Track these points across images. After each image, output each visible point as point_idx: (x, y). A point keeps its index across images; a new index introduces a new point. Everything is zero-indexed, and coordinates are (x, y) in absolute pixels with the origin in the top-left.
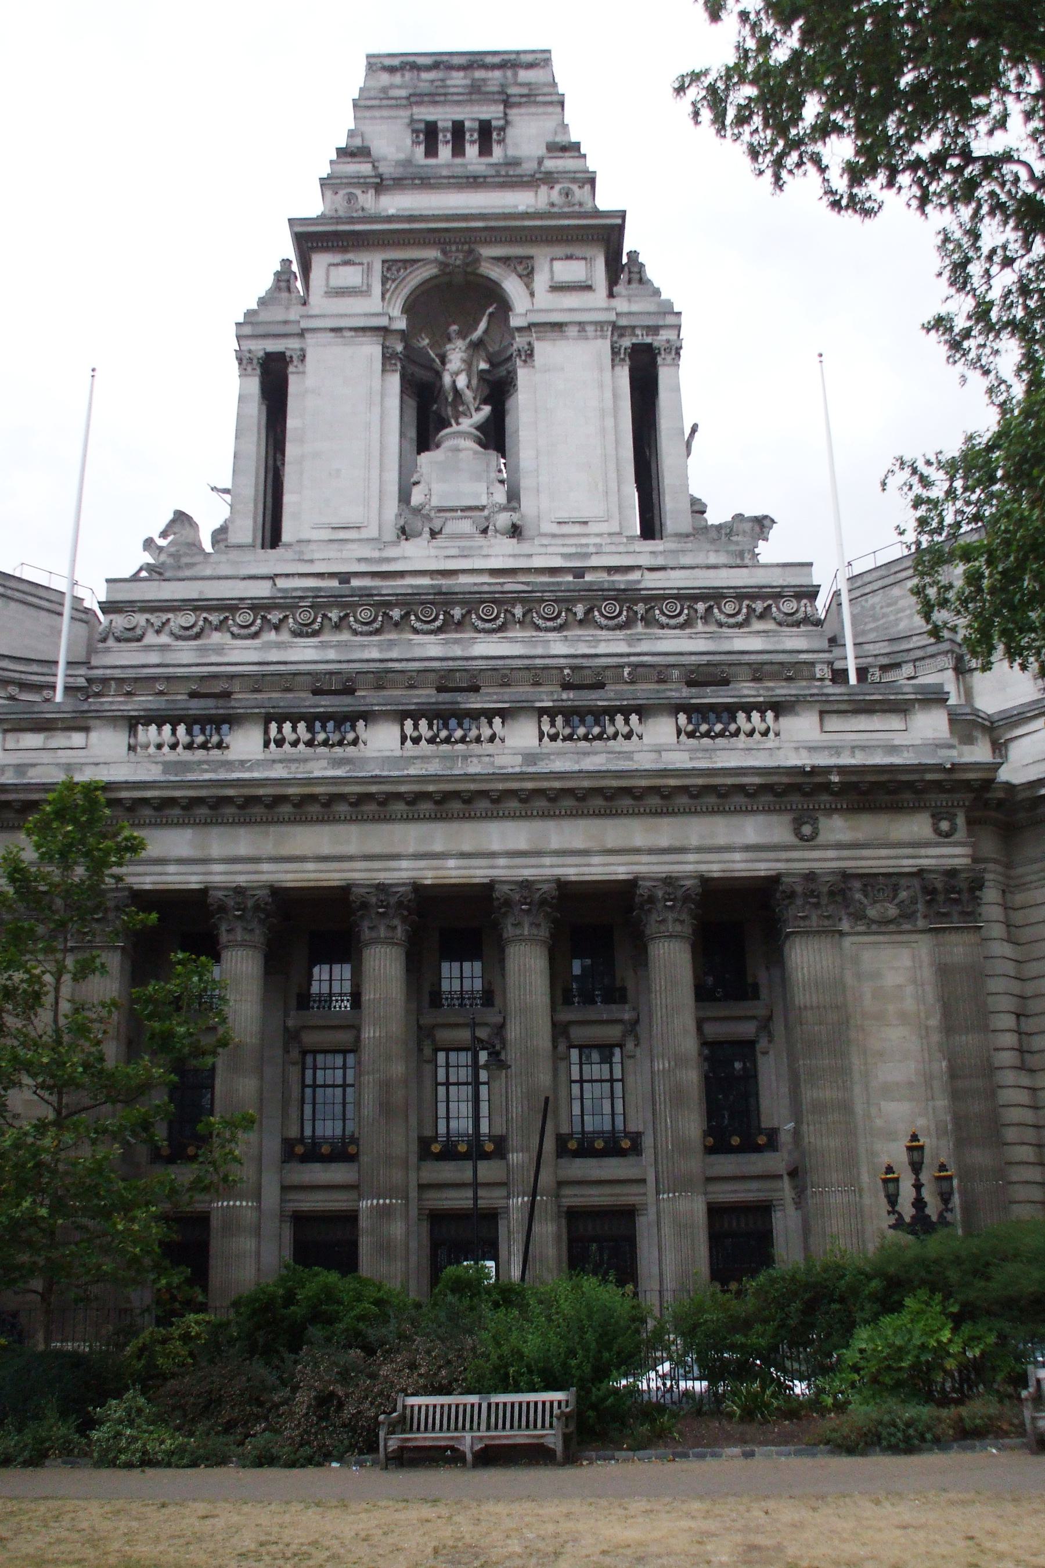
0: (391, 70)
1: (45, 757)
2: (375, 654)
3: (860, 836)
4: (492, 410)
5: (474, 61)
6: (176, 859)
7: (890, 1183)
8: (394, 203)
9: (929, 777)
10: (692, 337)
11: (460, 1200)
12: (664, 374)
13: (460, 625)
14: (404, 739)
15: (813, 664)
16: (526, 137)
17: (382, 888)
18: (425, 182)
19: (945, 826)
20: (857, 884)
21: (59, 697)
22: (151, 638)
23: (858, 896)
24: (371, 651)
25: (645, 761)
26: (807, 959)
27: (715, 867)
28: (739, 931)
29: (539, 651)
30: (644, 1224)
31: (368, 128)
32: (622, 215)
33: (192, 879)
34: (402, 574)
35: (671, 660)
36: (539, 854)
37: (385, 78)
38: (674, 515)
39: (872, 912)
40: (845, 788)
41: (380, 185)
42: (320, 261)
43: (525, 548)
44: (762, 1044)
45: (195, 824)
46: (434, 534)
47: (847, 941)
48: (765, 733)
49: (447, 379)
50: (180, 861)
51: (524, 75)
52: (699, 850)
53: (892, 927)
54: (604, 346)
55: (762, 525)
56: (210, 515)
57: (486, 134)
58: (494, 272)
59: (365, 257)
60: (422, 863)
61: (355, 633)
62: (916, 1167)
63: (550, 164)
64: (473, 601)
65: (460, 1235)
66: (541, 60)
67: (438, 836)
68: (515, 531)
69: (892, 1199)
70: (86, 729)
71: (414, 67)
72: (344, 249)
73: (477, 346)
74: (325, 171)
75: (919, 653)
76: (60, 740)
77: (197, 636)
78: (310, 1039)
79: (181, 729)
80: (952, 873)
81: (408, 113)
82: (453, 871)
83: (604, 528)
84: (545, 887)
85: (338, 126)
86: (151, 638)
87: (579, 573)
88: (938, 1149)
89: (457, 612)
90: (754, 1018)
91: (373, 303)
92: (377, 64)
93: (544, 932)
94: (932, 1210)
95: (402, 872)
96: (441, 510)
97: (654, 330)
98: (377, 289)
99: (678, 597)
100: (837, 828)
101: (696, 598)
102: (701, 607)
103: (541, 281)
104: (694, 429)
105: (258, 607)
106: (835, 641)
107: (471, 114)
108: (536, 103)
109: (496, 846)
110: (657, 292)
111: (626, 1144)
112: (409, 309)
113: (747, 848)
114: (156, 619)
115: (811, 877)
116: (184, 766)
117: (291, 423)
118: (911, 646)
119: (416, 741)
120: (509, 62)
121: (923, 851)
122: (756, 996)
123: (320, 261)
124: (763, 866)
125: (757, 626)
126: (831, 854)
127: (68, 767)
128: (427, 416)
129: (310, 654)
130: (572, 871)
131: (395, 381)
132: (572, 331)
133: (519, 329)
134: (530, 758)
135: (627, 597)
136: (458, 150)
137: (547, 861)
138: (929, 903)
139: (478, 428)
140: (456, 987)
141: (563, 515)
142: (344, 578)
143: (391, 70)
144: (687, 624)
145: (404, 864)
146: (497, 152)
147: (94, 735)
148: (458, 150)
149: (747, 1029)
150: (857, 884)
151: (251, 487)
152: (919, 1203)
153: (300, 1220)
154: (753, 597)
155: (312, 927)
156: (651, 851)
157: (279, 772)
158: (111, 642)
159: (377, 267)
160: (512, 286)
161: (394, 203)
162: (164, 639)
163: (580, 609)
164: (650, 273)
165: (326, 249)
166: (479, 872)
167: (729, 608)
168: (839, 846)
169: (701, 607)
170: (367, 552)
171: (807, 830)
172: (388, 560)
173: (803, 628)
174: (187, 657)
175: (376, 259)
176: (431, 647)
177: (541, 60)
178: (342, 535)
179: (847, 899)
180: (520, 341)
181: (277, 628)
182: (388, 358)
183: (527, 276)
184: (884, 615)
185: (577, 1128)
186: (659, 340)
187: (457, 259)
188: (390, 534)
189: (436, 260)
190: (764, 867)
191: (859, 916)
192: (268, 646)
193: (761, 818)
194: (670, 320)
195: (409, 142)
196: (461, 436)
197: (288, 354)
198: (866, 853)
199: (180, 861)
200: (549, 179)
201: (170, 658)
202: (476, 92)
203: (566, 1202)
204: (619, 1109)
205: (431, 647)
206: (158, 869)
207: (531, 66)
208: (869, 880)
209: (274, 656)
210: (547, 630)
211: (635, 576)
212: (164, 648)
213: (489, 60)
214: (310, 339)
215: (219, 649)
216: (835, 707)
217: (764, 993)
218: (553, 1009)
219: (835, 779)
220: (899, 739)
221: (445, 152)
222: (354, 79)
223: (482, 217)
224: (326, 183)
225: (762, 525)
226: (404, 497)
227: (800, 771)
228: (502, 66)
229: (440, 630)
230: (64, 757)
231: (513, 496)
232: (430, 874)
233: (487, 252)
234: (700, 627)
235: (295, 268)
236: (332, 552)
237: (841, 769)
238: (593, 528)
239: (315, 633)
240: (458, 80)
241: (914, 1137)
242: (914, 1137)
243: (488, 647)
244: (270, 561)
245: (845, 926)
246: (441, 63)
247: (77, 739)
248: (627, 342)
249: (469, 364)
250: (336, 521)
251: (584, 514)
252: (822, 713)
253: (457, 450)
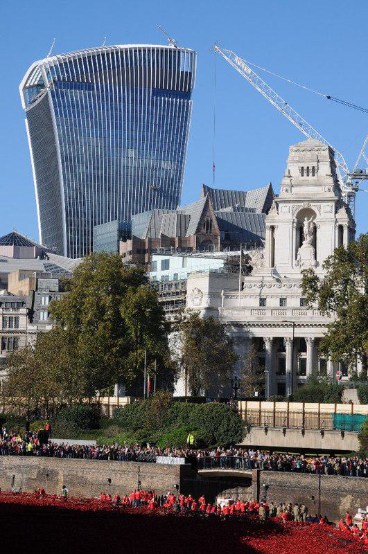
49: (304, 230)
107: (311, 165)
123: (280, 205)
131: (294, 232)
136: (308, 175)
146: (316, 174)
148: (308, 175)
221: (305, 174)
230: (241, 315)
231: (316, 258)
233: (312, 204)
248: (337, 224)
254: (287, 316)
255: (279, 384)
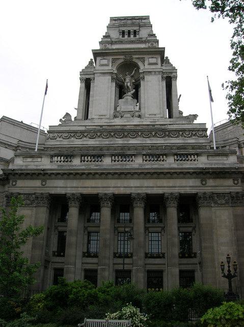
0: (115, 20)
1: (32, 163)
2: (107, 143)
3: (216, 184)
4: (136, 91)
5: (133, 18)
6: (60, 187)
7: (222, 266)
8: (115, 47)
9: (232, 170)
10: (180, 74)
11: (120, 267)
12: (173, 82)
13: (126, 137)
14: (112, 160)
15: (206, 146)
16: (143, 33)
17: (105, 194)
18: (121, 42)
19: (236, 182)
20: (216, 195)
21: (36, 150)
22: (58, 139)
23: (216, 198)
24: (106, 142)
25: (167, 166)
26: (203, 212)
27: (182, 191)
28: (188, 205)
29: (144, 143)
30: (165, 274)
31: (110, 32)
32: (164, 48)
33: (63, 191)
34: (114, 125)
35: (173, 145)
36: (142, 187)
37: (114, 22)
38: (175, 114)
39: (219, 202)
40: (213, 173)
41: (112, 43)
42: (98, 59)
43: (142, 120)
44: (193, 233)
45: (64, 179)
46: (122, 117)
47: (213, 208)
48: (195, 160)
49: (126, 84)
50: (60, 187)
51: (143, 21)
52: (179, 187)
53: (223, 206)
54: (160, 76)
55: (195, 116)
56: (74, 114)
57: (135, 33)
58: (136, 61)
59: (108, 58)
60: (115, 189)
61: (103, 138)
62: (229, 262)
63: (148, 38)
64: (130, 131)
65: (123, 275)
66: (147, 18)
67: (119, 183)
68: (140, 116)
69: (223, 270)
70: (41, 157)
71: (120, 20)
72: (104, 56)
73: (132, 77)
74: (100, 40)
75: (230, 144)
76: (35, 160)
77: (68, 138)
78: (90, 229)
79: (62, 158)
80: (237, 193)
82: (122, 191)
83: (159, 116)
84: (143, 195)
85: (103, 31)
86: (58, 139)
87: (154, 125)
88: (234, 258)
89: (126, 134)
90: (191, 227)
91: (110, 67)
92: (112, 19)
93: (143, 205)
94: (232, 272)
95: (110, 191)
96: (123, 112)
97: (171, 73)
98: (111, 65)
99: (175, 131)
100: (211, 182)
101: (180, 131)
102: (181, 133)
103: (146, 63)
104: (180, 96)
105: (82, 132)
106: (212, 141)
107: (132, 29)
108: (146, 26)
109: (132, 185)
110: (172, 65)
111: (161, 255)
112: (118, 69)
113: (190, 187)
114: (60, 135)
115: (205, 193)
116: (62, 166)
117: (91, 93)
119: (115, 161)
120: (141, 18)
121: (231, 188)
122: (192, 222)
123: (98, 59)
124: (194, 191)
125: (193, 137)
126: (210, 188)
127: (37, 166)
128: (121, 91)
129: (93, 143)
130: (149, 191)
131: (114, 84)
133: (141, 73)
134: (140, 165)
135: (164, 131)
136: (129, 36)
137: (144, 189)
138: (232, 200)
139: (133, 94)
140: (123, 218)
141: (150, 113)
142: (101, 126)
143: (115, 20)
144: (177, 137)
145: (111, 189)
146: (138, 36)
147: (43, 159)
148: (129, 36)
149: (190, 229)
150: (216, 195)
151: (82, 107)
152: (229, 271)
153: (86, 271)
154: (193, 131)
155: (90, 204)
156: (168, 187)
157: (83, 167)
158: (49, 140)
159: (111, 60)
160: (140, 64)
161: (115, 47)
162: (61, 139)
163: (153, 133)
164: (170, 61)
165: (100, 56)
166: (128, 191)
167: (187, 133)
168: (212, 186)
169: (181, 133)
170: (107, 121)
171: (204, 183)
172: (111, 122)
173: (204, 138)
174: (65, 143)
175: (110, 58)
176: (120, 141)
177: (147, 18)
178: (102, 117)
179: (213, 198)
180: (141, 76)
181: (86, 137)
182: (113, 79)
183: (143, 62)
185: (119, 251)
186: (172, 75)
187: (128, 58)
188: (112, 117)
189: (124, 58)
190: (194, 191)
191: (216, 203)
192: (84, 141)
193: (193, 180)
194: (175, 71)
196: (128, 97)
198: (217, 188)
199: (60, 187)
200: (148, 41)
201: (62, 143)
202: (133, 25)
203: (147, 269)
204: (119, 245)
205: (120, 141)
206: (56, 189)
207: (145, 19)
208: (218, 195)
209: (85, 143)
210: (146, 138)
211: (166, 126)
212: (61, 141)
213: (136, 18)
214: (96, 75)
215: (73, 141)
216: (211, 154)
217: (194, 221)
218: (145, 224)
220: (225, 162)
221: (126, 37)
222: (107, 22)
223: (134, 49)
224: (100, 43)
225: (195, 116)
226: (115, 109)
227: (203, 169)
228: (139, 19)
229: (122, 138)
230: (36, 163)
232: (117, 191)
233: (134, 56)
234: (181, 138)
235: (93, 61)
236: (99, 121)
237: (212, 168)
238: (157, 116)
239: (94, 138)
240: (129, 22)
241: (228, 255)
242: (228, 255)
243: (133, 141)
244: (87, 123)
245: (213, 205)
246: (126, 19)
247: (39, 160)
248: (165, 76)
249: (130, 80)
250: (100, 114)
251: (155, 113)
252: (208, 156)
253: (127, 99)
254: (104, 163)
255: (86, 271)
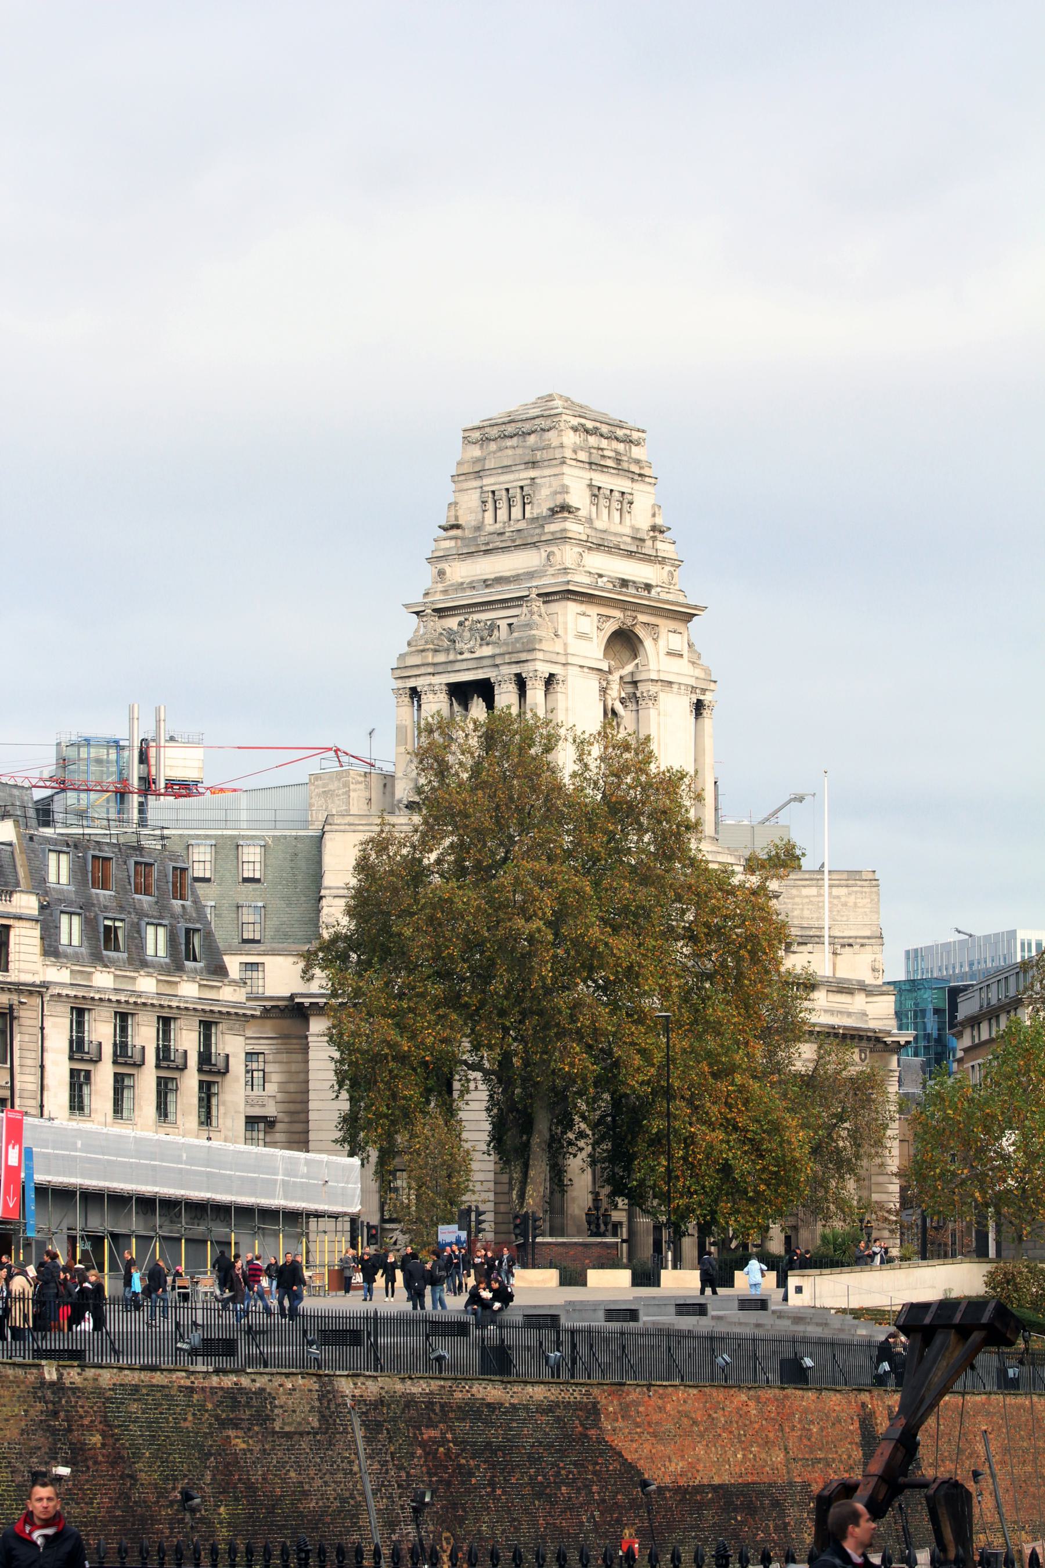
9: (869, 1034)
72: (582, 602)
81: (588, 475)
118: (811, 933)
132: (675, 686)
159: (596, 618)
160: (648, 643)
175: (593, 610)
184: (785, 903)
187: (629, 622)
195: (588, 502)
197: (558, 677)
200: (662, 561)
214: (572, 671)
219: (841, 1031)
233: (642, 618)
237: (845, 1028)
